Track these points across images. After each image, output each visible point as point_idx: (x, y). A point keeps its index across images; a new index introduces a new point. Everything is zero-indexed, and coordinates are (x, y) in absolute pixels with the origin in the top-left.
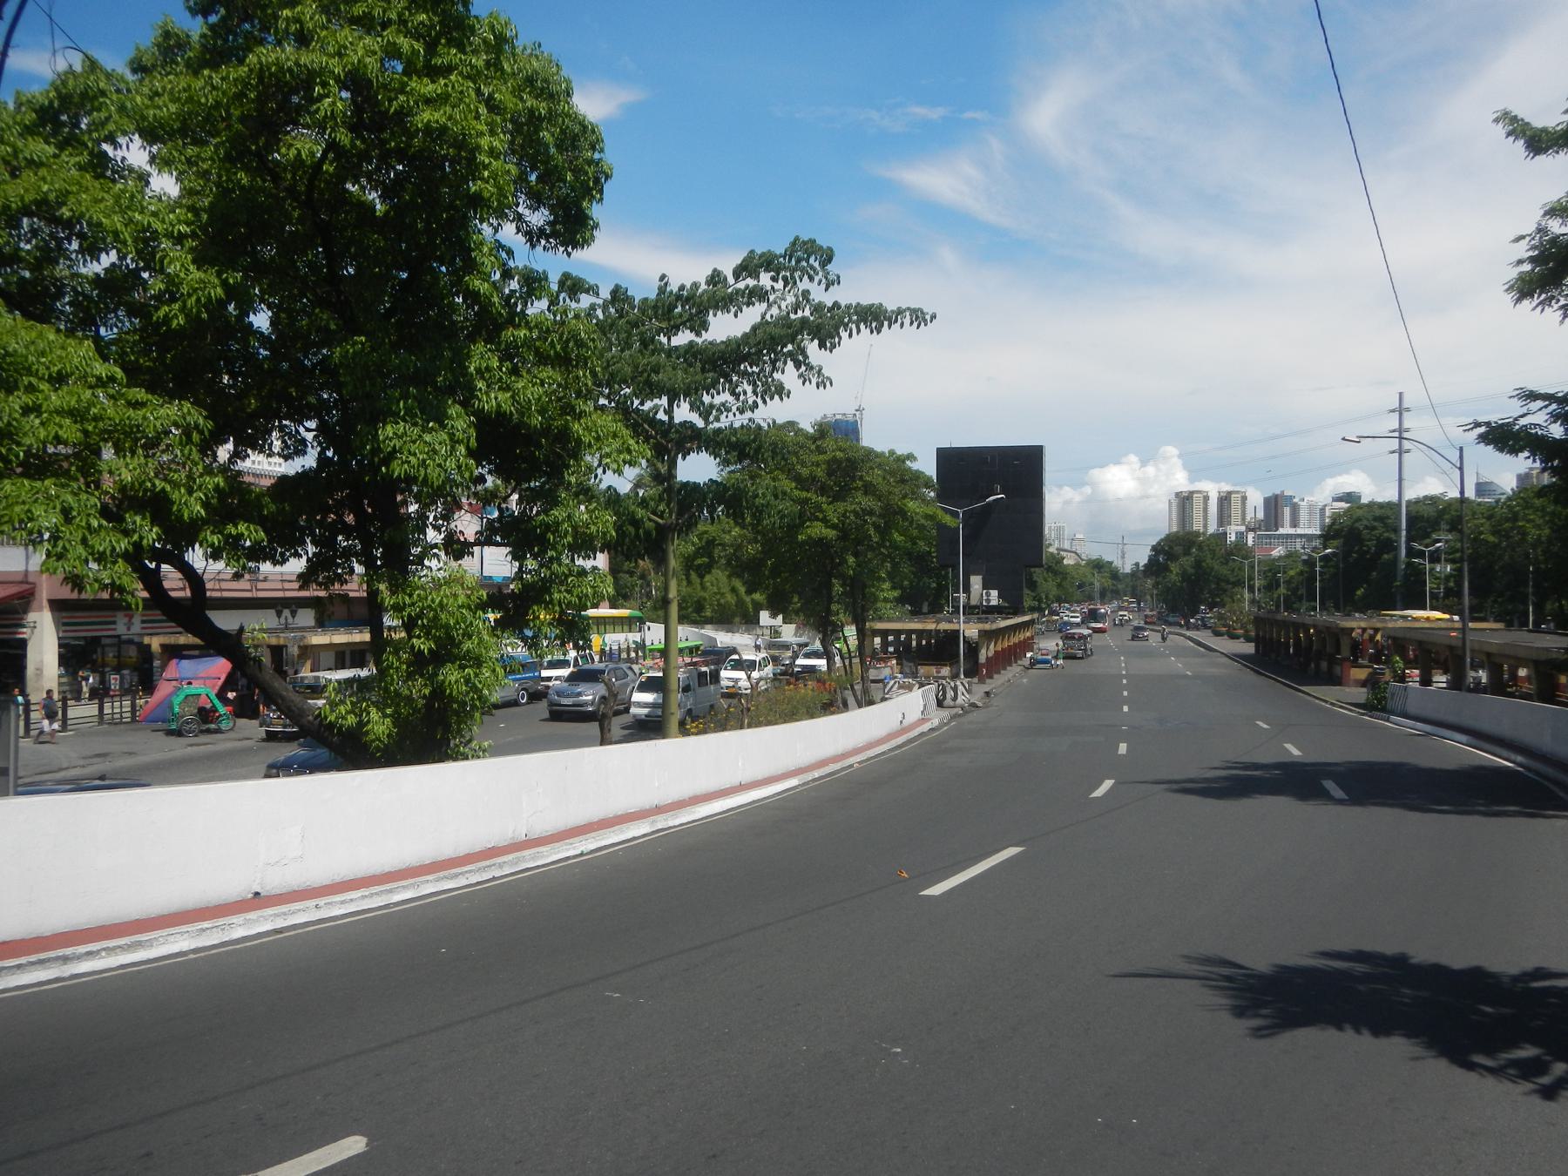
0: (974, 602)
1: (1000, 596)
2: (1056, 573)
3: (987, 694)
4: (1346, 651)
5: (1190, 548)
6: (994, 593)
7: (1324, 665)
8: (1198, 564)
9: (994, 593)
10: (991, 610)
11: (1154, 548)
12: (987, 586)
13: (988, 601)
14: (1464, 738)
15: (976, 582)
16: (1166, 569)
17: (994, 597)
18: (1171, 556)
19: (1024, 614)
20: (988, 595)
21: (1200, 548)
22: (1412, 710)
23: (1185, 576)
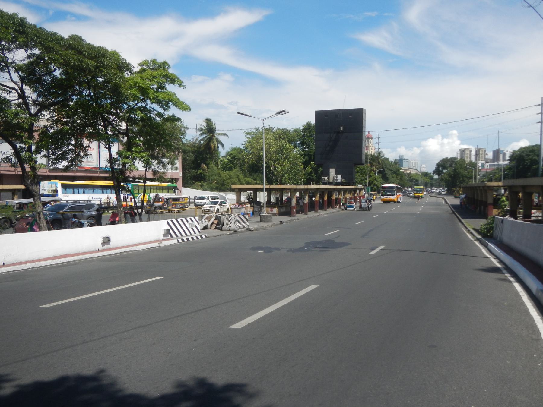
0: (331, 181)
1: (342, 178)
2: (397, 174)
3: (281, 222)
4: (490, 201)
5: (452, 164)
6: (340, 176)
7: (482, 207)
8: (455, 171)
9: (340, 176)
10: (338, 184)
11: (437, 164)
12: (337, 173)
13: (337, 180)
14: (533, 284)
15: (332, 171)
16: (442, 172)
17: (340, 178)
18: (444, 168)
19: (353, 185)
20: (337, 177)
21: (456, 164)
22: (506, 239)
23: (449, 175)
